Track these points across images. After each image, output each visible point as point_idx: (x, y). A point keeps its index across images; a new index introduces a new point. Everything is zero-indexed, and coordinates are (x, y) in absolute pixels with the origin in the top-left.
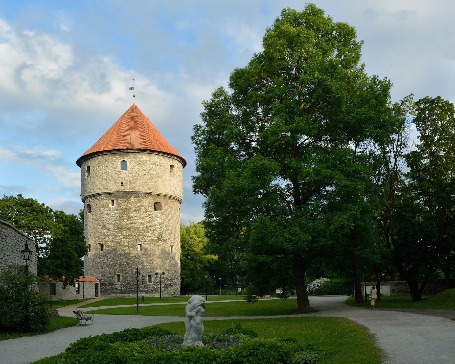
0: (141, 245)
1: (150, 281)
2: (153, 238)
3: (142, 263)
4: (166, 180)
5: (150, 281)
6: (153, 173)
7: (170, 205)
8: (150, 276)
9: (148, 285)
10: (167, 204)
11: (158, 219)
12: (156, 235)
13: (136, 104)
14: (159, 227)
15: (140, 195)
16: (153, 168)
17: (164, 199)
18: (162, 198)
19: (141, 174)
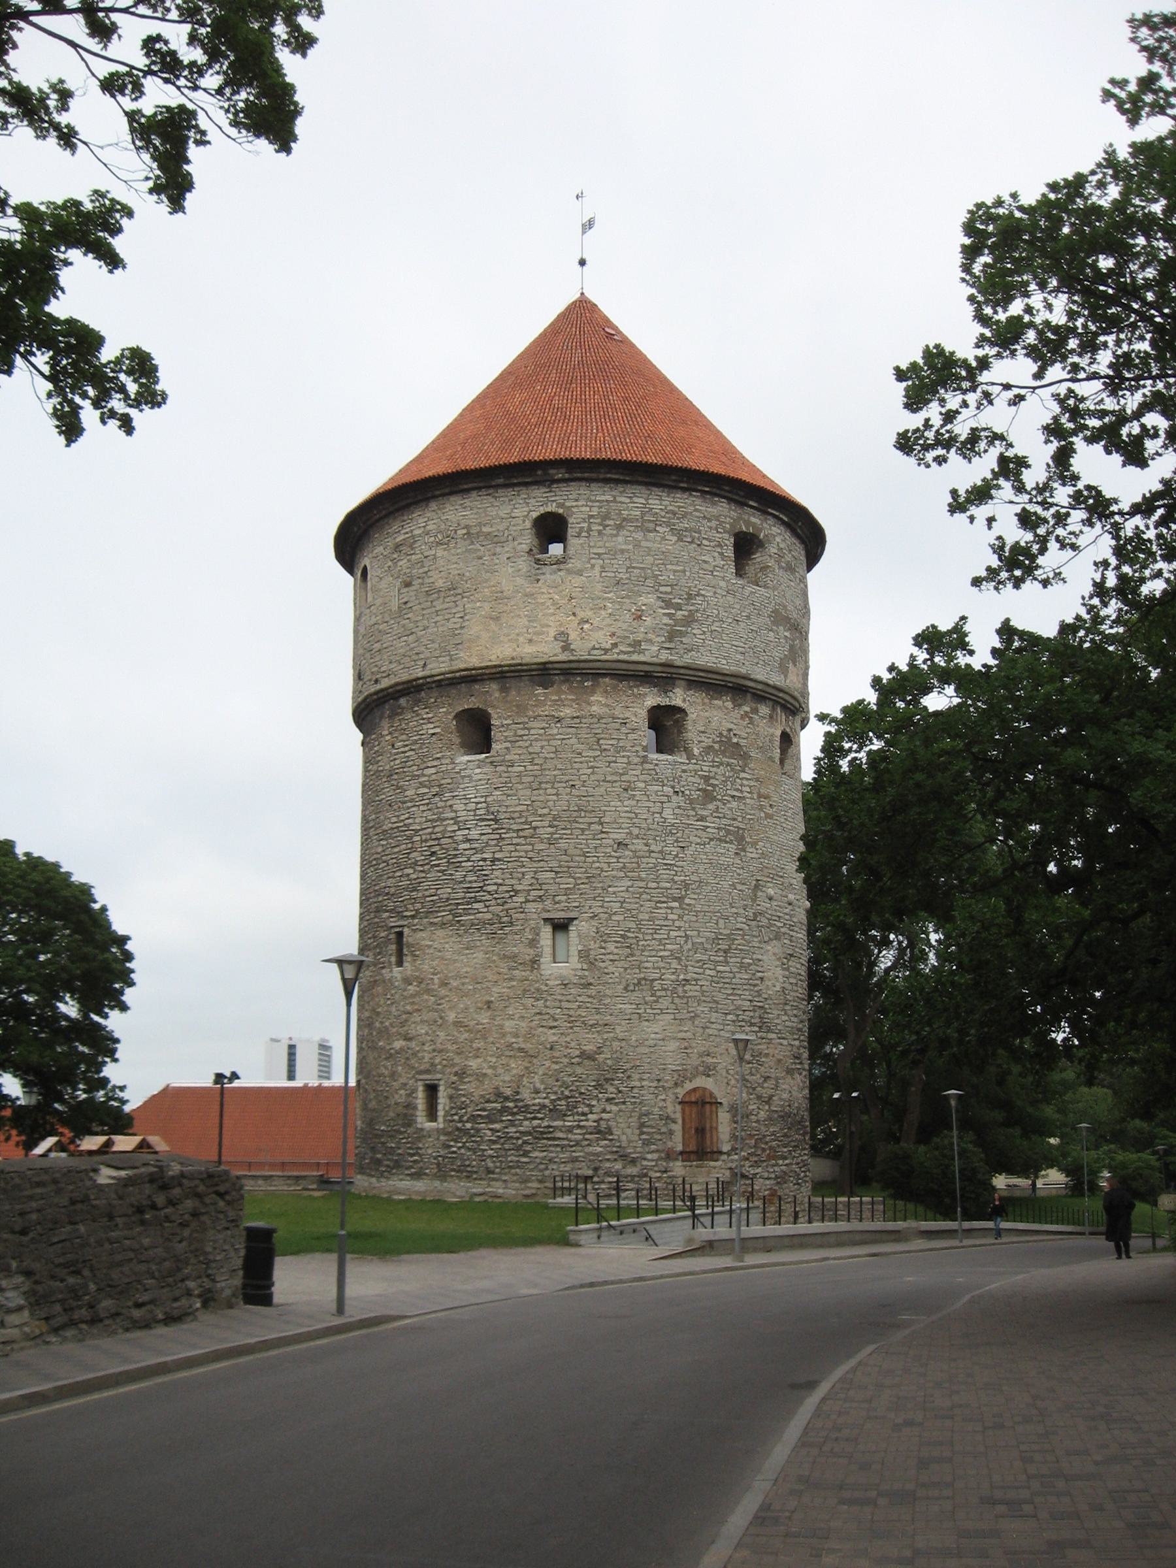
0: (400, 935)
1: (432, 1114)
2: (445, 892)
3: (403, 1024)
4: (499, 597)
5: (432, 1114)
6: (440, 583)
7: (547, 710)
8: (432, 1090)
9: (421, 1134)
10: (521, 709)
11: (471, 792)
12: (458, 876)
13: (592, 296)
14: (474, 833)
15: (403, 701)
16: (441, 562)
17: (504, 689)
18: (494, 686)
19: (394, 605)
